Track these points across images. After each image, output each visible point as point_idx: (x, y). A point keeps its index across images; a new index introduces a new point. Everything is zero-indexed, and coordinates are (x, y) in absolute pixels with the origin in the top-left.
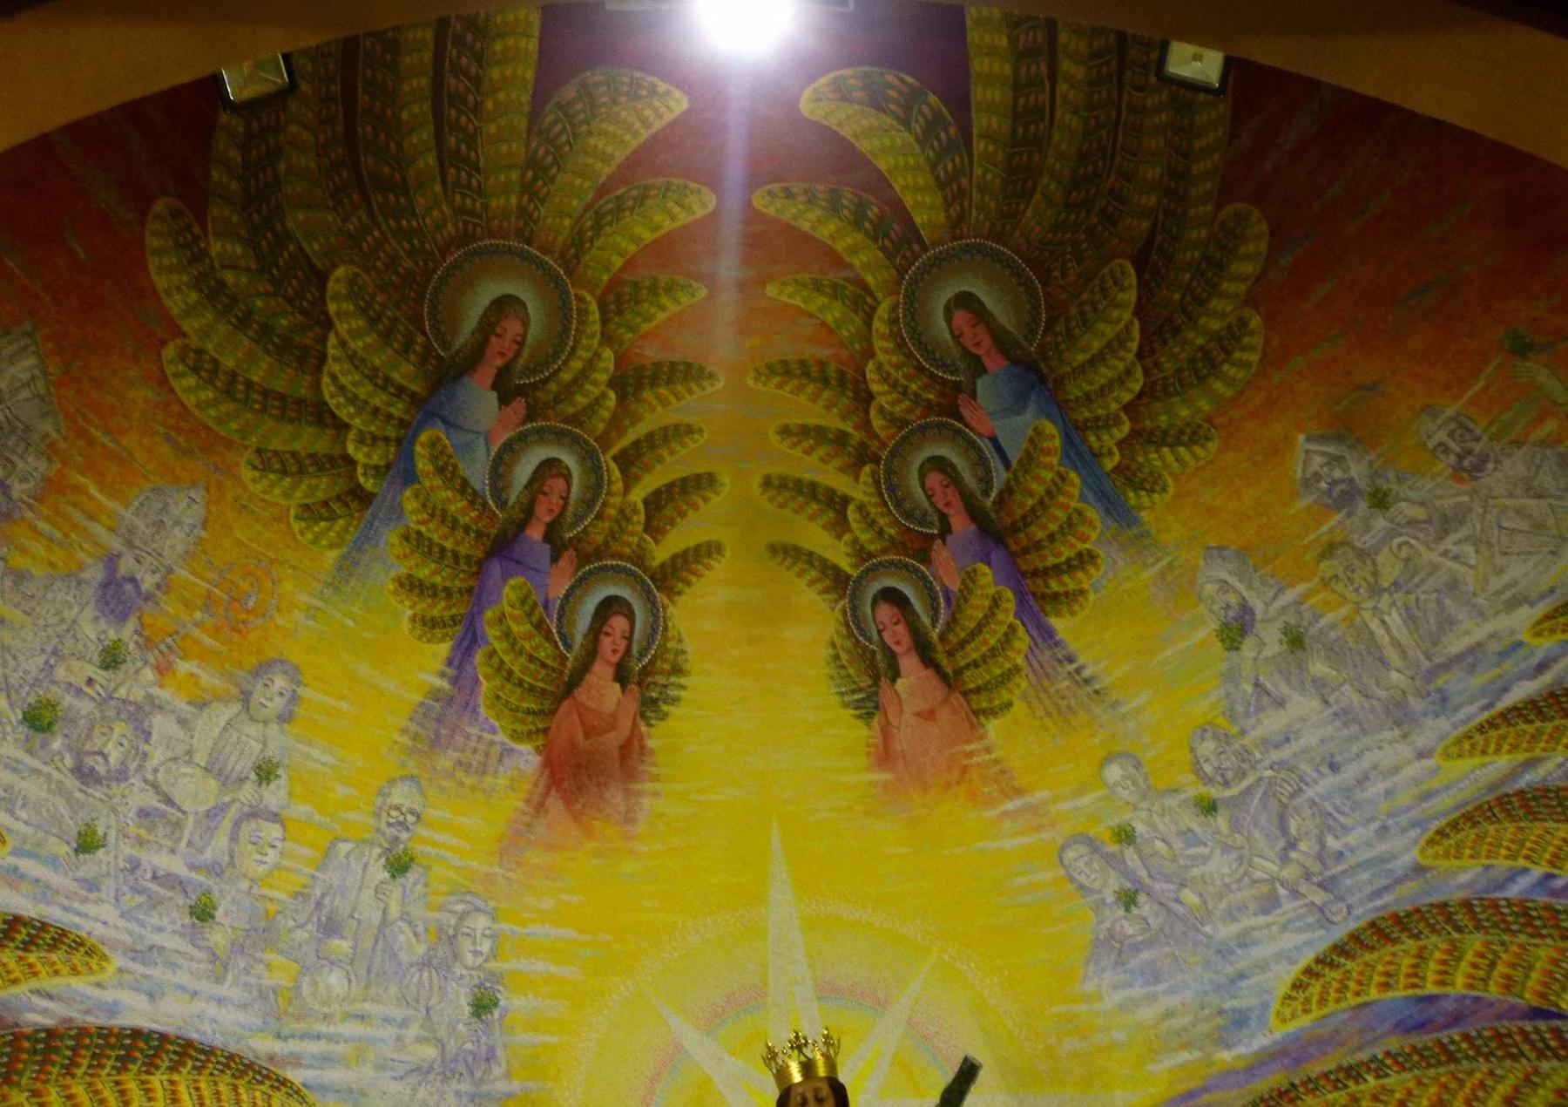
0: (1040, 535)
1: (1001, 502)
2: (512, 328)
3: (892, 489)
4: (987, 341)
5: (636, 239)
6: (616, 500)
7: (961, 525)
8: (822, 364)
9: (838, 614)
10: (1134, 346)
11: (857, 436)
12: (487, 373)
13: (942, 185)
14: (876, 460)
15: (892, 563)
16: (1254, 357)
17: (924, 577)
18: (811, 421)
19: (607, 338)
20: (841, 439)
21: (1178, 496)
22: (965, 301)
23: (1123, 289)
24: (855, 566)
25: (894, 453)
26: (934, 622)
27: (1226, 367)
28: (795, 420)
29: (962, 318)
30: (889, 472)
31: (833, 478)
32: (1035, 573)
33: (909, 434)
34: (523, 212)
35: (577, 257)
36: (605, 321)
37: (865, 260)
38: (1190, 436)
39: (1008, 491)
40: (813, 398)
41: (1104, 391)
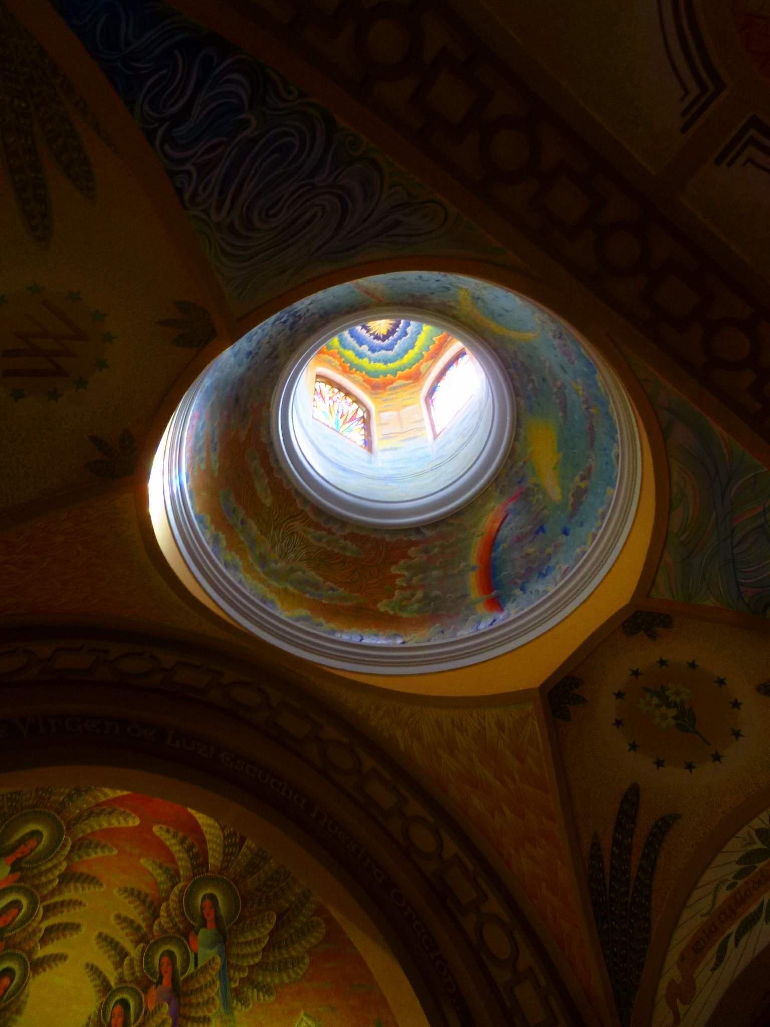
0: (194, 1001)
1: (186, 980)
2: (32, 843)
3: (147, 956)
4: (212, 915)
5: (100, 825)
6: (35, 925)
7: (166, 981)
8: (146, 896)
9: (100, 1001)
10: (263, 945)
11: (145, 929)
12: (12, 858)
13: (225, 854)
14: (147, 943)
15: (132, 988)
16: (301, 973)
17: (141, 999)
18: (131, 917)
19: (68, 858)
20: (139, 928)
21: (251, 1012)
22: (212, 897)
23: (270, 923)
24: (116, 984)
25: (155, 943)
26: (136, 1020)
27: (290, 970)
28: (124, 914)
29: (208, 902)
30: (150, 949)
31: (127, 944)
32: (184, 1017)
33: (165, 938)
34: (63, 802)
35: (74, 825)
36: (71, 851)
37: (183, 864)
38: (266, 990)
39: (191, 977)
40: (136, 908)
41: (245, 956)
